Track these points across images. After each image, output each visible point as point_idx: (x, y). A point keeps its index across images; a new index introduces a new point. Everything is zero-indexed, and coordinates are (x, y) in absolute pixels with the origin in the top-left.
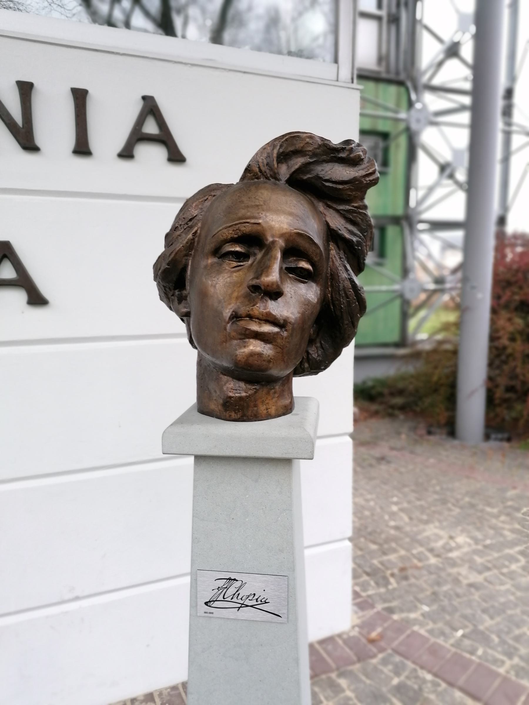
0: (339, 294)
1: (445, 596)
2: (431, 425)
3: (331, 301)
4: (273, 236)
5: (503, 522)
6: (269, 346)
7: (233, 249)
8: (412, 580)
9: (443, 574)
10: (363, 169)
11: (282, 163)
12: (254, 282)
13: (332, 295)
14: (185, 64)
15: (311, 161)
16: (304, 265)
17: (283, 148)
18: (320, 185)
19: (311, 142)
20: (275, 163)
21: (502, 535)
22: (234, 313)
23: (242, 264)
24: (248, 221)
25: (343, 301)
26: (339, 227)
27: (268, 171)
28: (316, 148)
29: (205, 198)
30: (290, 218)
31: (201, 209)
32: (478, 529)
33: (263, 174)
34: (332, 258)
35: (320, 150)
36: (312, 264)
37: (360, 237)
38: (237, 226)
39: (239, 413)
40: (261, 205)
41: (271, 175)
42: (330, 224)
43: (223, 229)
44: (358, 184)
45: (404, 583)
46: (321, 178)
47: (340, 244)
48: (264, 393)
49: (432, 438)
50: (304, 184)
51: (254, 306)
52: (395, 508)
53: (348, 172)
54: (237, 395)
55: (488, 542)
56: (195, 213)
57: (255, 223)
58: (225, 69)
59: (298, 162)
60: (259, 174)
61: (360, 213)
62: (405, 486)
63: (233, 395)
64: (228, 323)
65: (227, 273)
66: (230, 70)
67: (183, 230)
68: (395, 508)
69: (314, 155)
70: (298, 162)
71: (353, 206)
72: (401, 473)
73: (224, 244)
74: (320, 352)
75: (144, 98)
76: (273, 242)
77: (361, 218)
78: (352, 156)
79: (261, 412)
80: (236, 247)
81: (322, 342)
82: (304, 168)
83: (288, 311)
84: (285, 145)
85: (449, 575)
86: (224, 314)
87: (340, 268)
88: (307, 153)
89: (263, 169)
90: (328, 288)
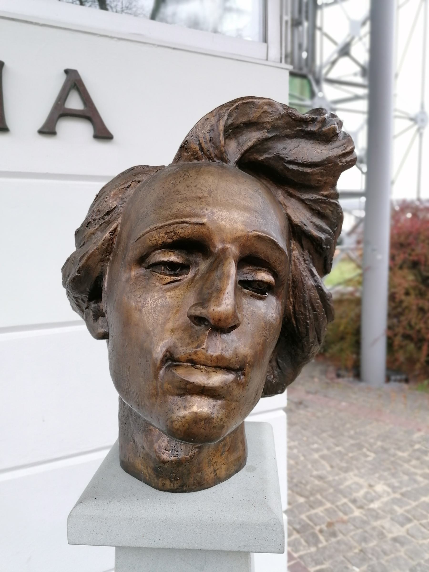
0: (304, 306)
1: (373, 554)
2: (339, 369)
3: (292, 314)
4: (223, 241)
5: (415, 467)
6: (219, 402)
7: (165, 259)
8: (340, 537)
9: (368, 528)
10: (338, 147)
11: (231, 139)
12: (199, 311)
13: (294, 307)
14: (112, 37)
15: (270, 135)
16: (265, 276)
17: (233, 118)
18: (281, 168)
19: (270, 110)
20: (222, 137)
21: (415, 481)
22: (168, 354)
23: (179, 278)
24: (187, 220)
25: (310, 315)
26: (305, 222)
27: (211, 150)
28: (277, 119)
29: (127, 185)
30: (247, 215)
31: (122, 199)
32: (394, 475)
33: (205, 154)
34: (294, 261)
35: (282, 122)
36: (275, 275)
37: (329, 234)
38: (172, 227)
39: (176, 482)
40: (206, 198)
41: (216, 155)
42: (293, 218)
43: (151, 230)
44: (332, 166)
45: (333, 540)
46: (282, 159)
47: (304, 242)
48: (210, 450)
49: (340, 380)
50: (261, 168)
51: (198, 347)
52: (316, 456)
53: (319, 151)
54: (173, 458)
55: (404, 489)
56: (114, 204)
57: (197, 224)
58: (154, 45)
59: (252, 137)
60: (200, 153)
61: (331, 204)
62: (324, 431)
63: (168, 459)
64: (160, 368)
65: (157, 292)
66: (159, 46)
67: (97, 226)
68: (316, 456)
69: (275, 128)
70: (252, 137)
71: (322, 195)
72: (318, 418)
73: (153, 251)
74: (276, 372)
75: (67, 72)
76: (224, 251)
77: (332, 209)
78: (325, 129)
79: (206, 477)
80: (170, 256)
81: (279, 360)
82: (260, 146)
84: (235, 115)
85: (374, 528)
86: (155, 355)
87: (305, 274)
88: (265, 125)
89: (205, 146)
90: (289, 299)
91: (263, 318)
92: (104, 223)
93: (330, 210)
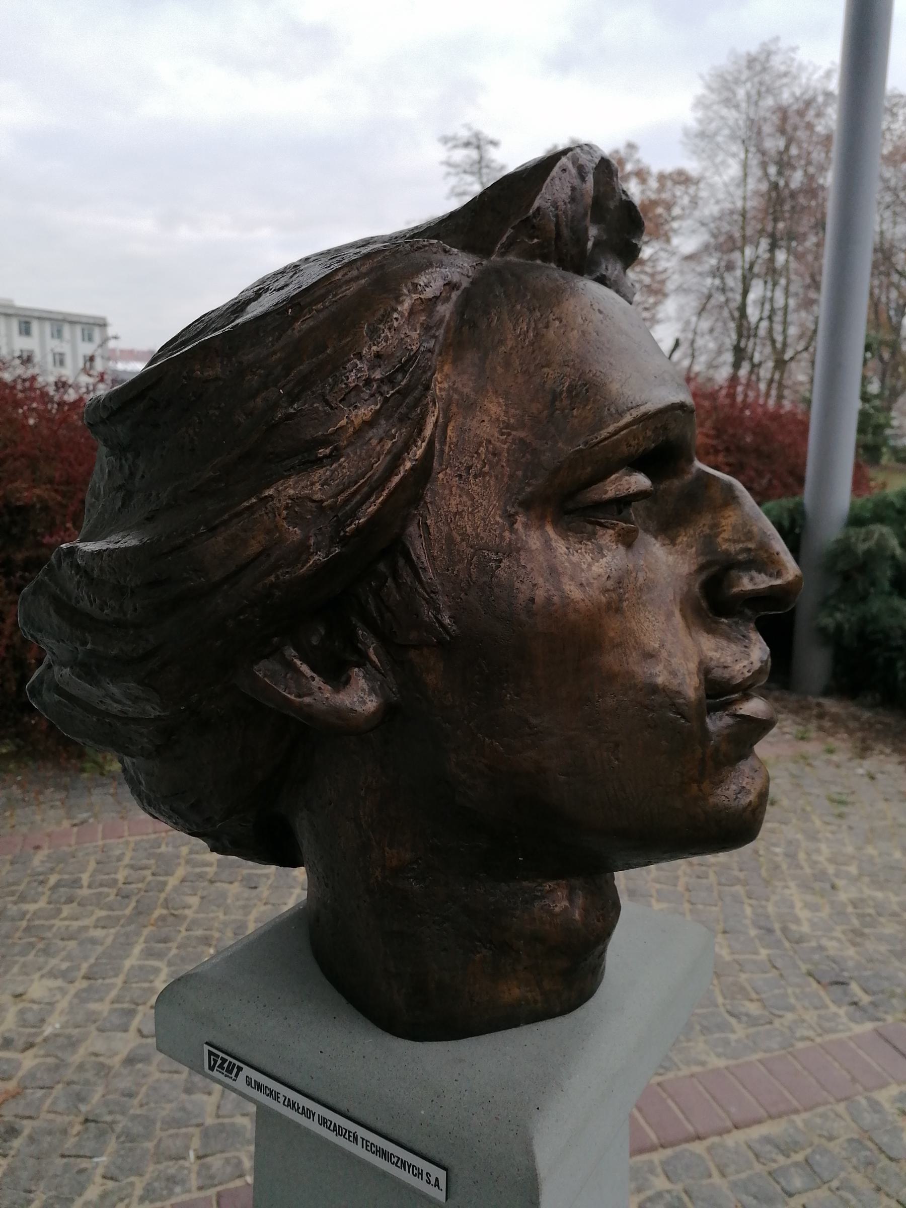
1: (111, 1113)
8: (27, 1127)
9: (69, 1074)
21: (94, 942)
32: (46, 952)
55: (85, 967)
85: (81, 1067)
92: (398, 392)
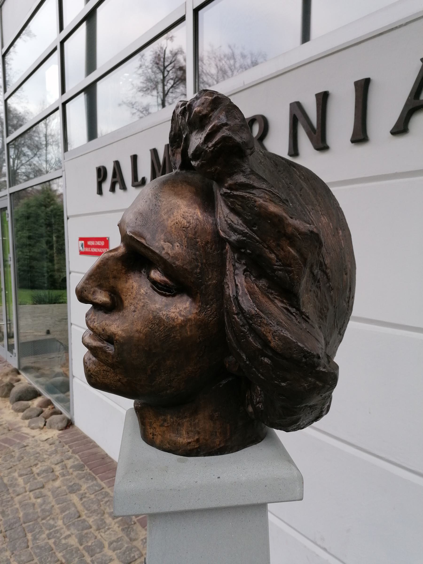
77: (240, 203)
83: (118, 327)
91: (153, 311)
93: (239, 205)
